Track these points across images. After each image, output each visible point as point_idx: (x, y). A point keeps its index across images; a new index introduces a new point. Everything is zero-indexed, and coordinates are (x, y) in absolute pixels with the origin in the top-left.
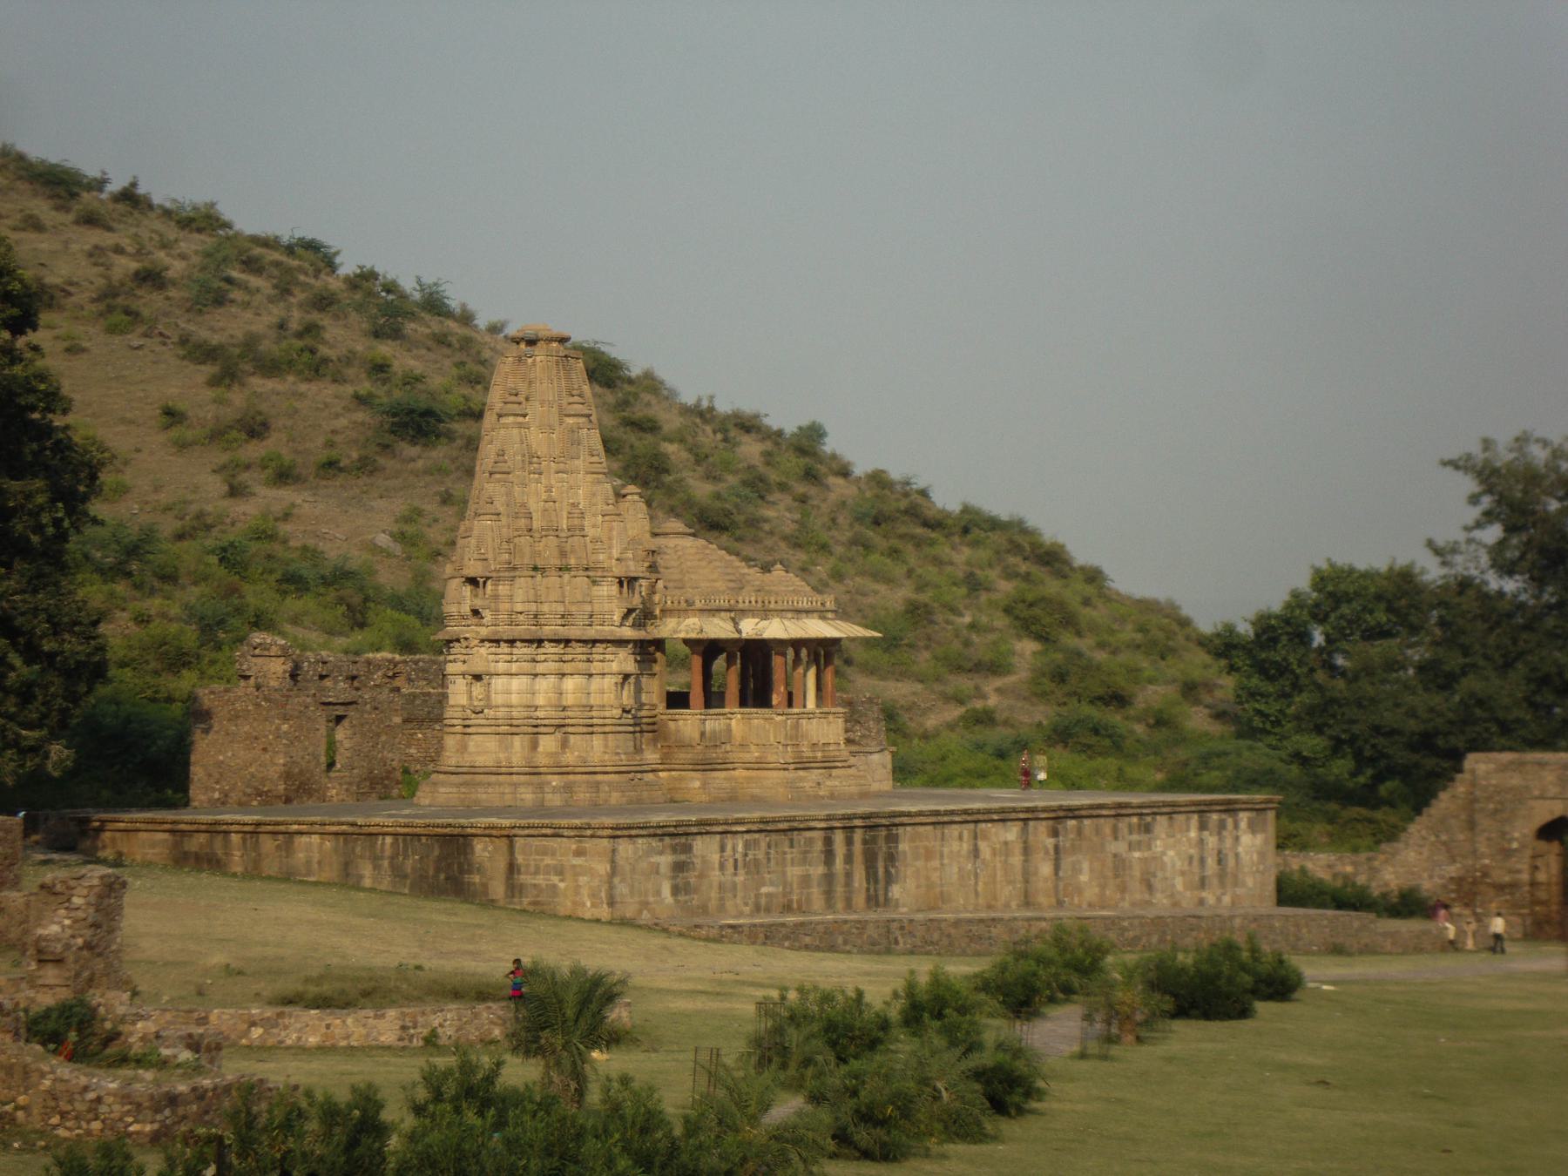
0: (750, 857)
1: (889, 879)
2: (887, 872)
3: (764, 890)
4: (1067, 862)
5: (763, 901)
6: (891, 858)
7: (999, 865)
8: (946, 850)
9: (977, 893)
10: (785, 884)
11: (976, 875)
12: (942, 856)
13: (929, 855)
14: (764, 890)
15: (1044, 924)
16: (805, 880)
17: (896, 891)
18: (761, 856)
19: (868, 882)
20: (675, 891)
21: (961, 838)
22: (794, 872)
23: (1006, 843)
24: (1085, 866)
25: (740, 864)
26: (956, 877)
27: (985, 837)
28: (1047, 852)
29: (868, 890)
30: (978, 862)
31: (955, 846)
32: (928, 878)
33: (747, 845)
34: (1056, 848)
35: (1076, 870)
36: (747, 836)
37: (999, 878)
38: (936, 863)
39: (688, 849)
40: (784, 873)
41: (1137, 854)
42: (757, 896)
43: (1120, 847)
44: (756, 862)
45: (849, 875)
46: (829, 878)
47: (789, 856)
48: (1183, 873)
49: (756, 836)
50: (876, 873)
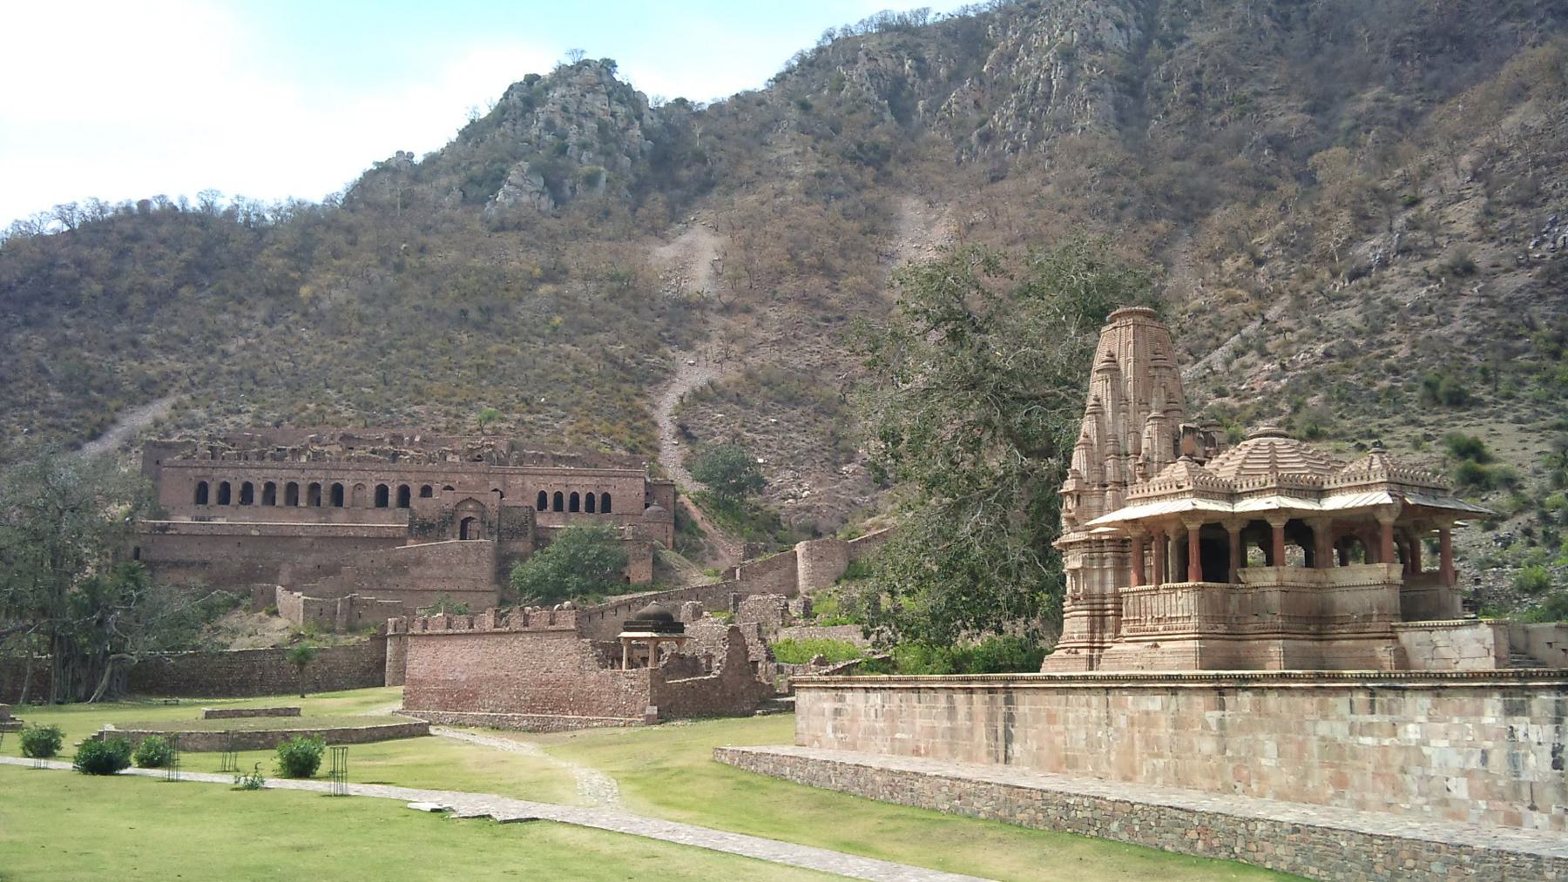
1: (1009, 739)
2: (1007, 731)
4: (1237, 742)
6: (1010, 718)
8: (1071, 716)
9: (1109, 763)
11: (1109, 744)
12: (1066, 721)
13: (1051, 718)
14: (898, 736)
20: (835, 730)
23: (1147, 713)
24: (1270, 747)
26: (1083, 743)
27: (1122, 706)
28: (1206, 726)
31: (1083, 711)
32: (1052, 742)
34: (1221, 723)
35: (1255, 752)
37: (1137, 749)
38: (1060, 727)
39: (842, 699)
41: (1368, 741)
43: (1334, 728)
45: (971, 731)
48: (1467, 774)
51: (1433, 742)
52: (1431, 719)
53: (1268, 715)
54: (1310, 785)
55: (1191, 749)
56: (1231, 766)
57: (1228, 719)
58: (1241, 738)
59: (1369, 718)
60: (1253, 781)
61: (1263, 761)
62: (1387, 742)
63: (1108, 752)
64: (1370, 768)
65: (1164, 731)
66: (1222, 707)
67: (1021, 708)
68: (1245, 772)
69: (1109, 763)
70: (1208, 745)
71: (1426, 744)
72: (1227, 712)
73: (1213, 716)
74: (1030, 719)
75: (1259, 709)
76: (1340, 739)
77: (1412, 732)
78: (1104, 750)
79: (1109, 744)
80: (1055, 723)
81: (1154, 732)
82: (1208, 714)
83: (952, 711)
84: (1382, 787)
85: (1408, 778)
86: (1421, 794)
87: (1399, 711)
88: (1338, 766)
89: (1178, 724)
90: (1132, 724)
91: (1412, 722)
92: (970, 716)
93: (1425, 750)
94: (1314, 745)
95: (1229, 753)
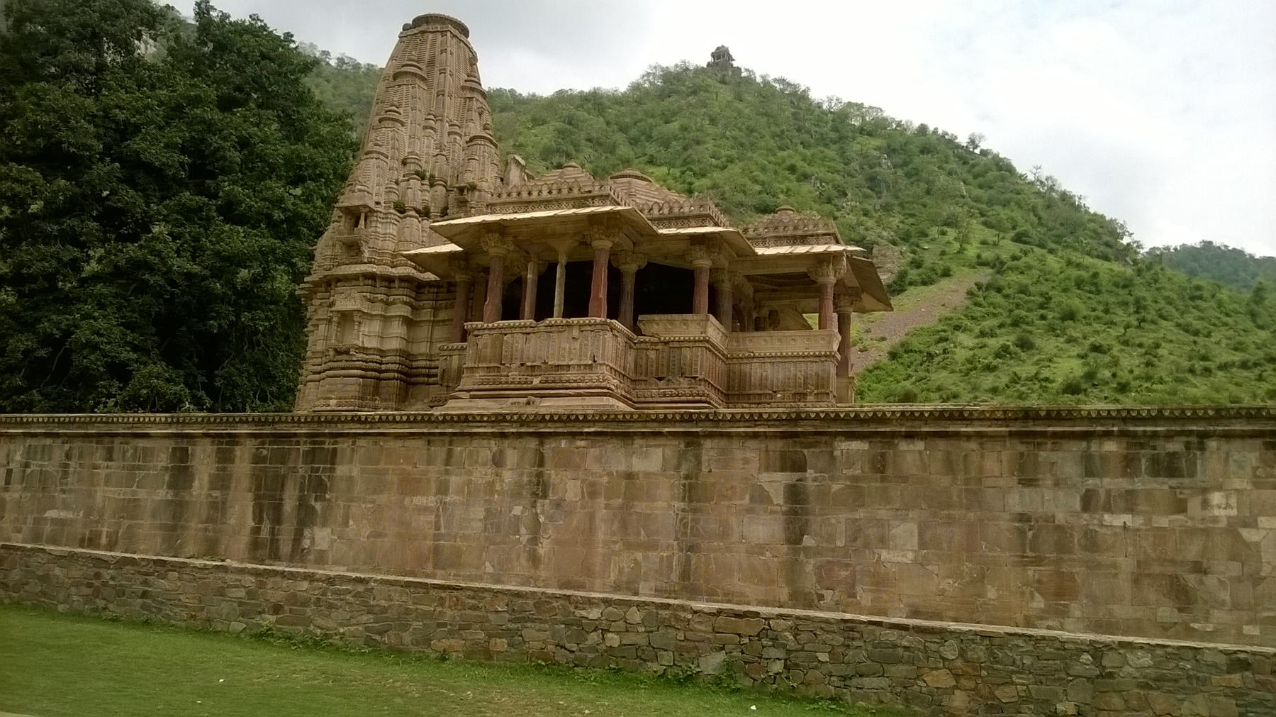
0: (34, 466)
1: (306, 517)
2: (303, 505)
3: (51, 514)
4: (832, 525)
5: (47, 529)
7: (602, 513)
8: (454, 480)
9: (534, 559)
10: (90, 510)
11: (536, 529)
12: (443, 489)
13: (410, 485)
14: (51, 514)
15: (305, 585)
16: (130, 508)
17: (321, 537)
18: (52, 467)
19: (258, 518)
21: (498, 461)
22: (107, 495)
23: (630, 476)
24: (906, 532)
25: (16, 475)
26: (478, 526)
27: (565, 463)
28: (761, 497)
29: (256, 531)
30: (543, 506)
31: (482, 474)
33: (29, 453)
34: (795, 494)
36: (29, 441)
37: (601, 533)
40: (91, 495)
42: (37, 521)
44: (44, 476)
45: (218, 509)
46: (178, 508)
47: (102, 473)
49: (48, 441)
50: (278, 508)
51: (1263, 521)
52: (1258, 484)
53: (904, 479)
54: (991, 593)
55: (724, 535)
56: (810, 566)
57: (811, 484)
58: (839, 520)
59: (1123, 484)
60: (859, 589)
61: (885, 555)
62: (1163, 522)
63: (534, 540)
64: (1126, 564)
65: (664, 506)
66: (798, 466)
67: (341, 470)
68: (844, 573)
69: (534, 559)
70: (765, 529)
71: (1251, 523)
72: (810, 473)
73: (776, 483)
74: (359, 488)
75: (879, 466)
76: (1061, 518)
77: (1221, 507)
78: (524, 536)
79: (536, 529)
80: (415, 493)
81: (641, 507)
82: (765, 477)
83: (181, 474)
84: (1152, 596)
85: (1211, 581)
86: (1236, 607)
87: (1192, 474)
88: (1058, 562)
89: (693, 492)
90: (593, 494)
91: (1219, 488)
92: (221, 481)
93: (1248, 535)
94: (1003, 526)
95: (808, 541)
